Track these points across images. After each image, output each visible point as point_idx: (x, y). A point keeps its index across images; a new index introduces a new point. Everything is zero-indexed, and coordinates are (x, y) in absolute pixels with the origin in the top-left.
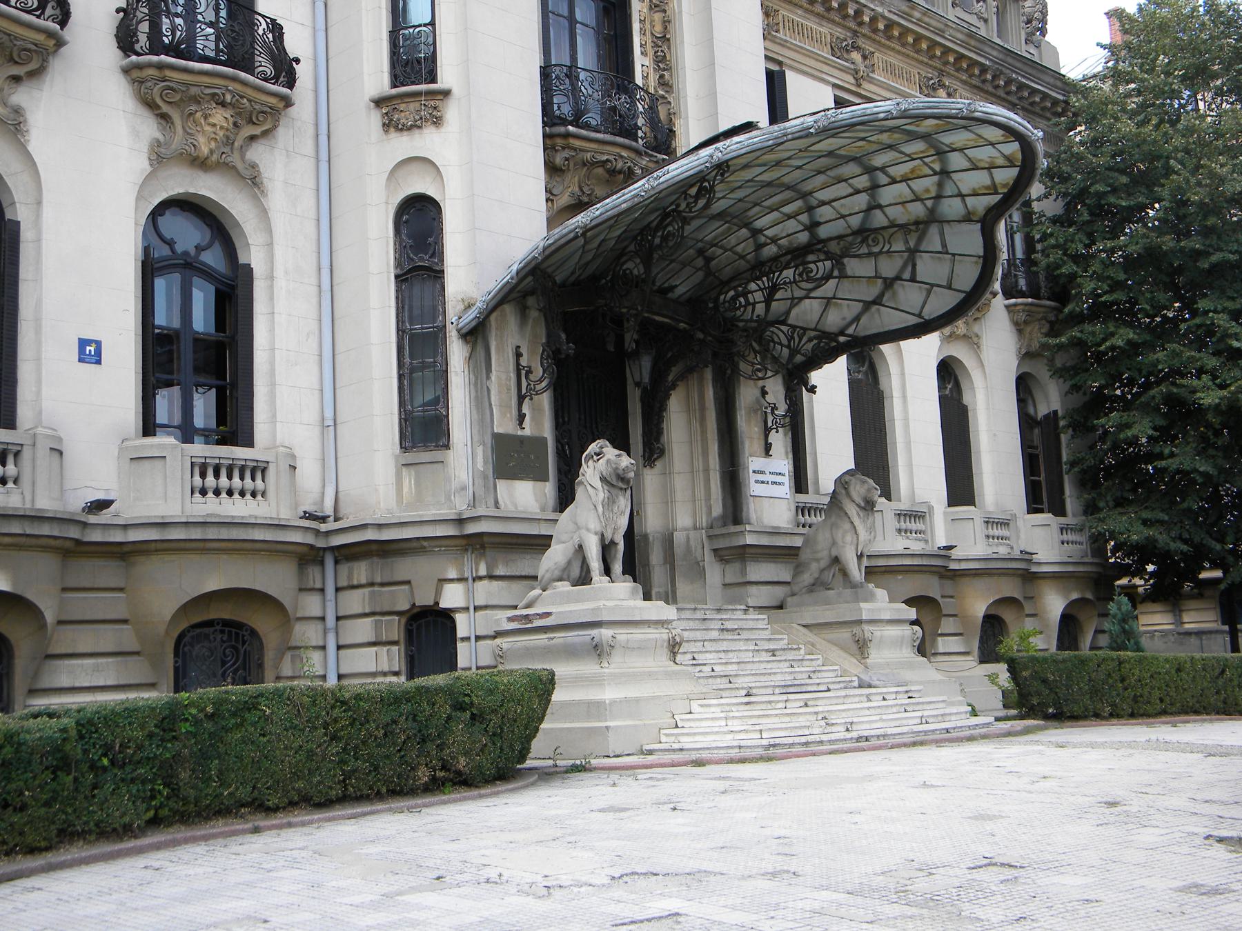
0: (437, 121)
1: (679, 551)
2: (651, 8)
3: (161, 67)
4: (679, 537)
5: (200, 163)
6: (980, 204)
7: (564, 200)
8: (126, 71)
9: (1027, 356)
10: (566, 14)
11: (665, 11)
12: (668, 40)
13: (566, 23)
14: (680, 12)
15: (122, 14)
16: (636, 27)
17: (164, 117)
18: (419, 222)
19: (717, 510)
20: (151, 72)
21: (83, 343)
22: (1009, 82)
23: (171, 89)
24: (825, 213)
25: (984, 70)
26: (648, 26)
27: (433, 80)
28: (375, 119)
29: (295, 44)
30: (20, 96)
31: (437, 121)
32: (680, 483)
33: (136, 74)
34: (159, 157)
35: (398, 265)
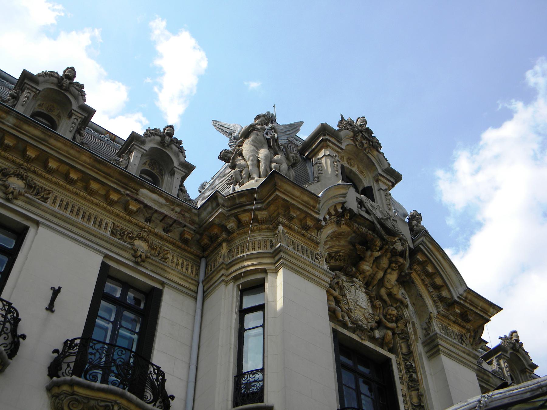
2: (409, 389)
3: (72, 384)
8: (49, 389)
10: (354, 387)
11: (418, 390)
12: (423, 407)
13: (354, 394)
14: (428, 389)
15: (56, 355)
16: (400, 399)
20: (65, 388)
23: (77, 400)
26: (408, 399)
29: (170, 388)
33: (56, 390)
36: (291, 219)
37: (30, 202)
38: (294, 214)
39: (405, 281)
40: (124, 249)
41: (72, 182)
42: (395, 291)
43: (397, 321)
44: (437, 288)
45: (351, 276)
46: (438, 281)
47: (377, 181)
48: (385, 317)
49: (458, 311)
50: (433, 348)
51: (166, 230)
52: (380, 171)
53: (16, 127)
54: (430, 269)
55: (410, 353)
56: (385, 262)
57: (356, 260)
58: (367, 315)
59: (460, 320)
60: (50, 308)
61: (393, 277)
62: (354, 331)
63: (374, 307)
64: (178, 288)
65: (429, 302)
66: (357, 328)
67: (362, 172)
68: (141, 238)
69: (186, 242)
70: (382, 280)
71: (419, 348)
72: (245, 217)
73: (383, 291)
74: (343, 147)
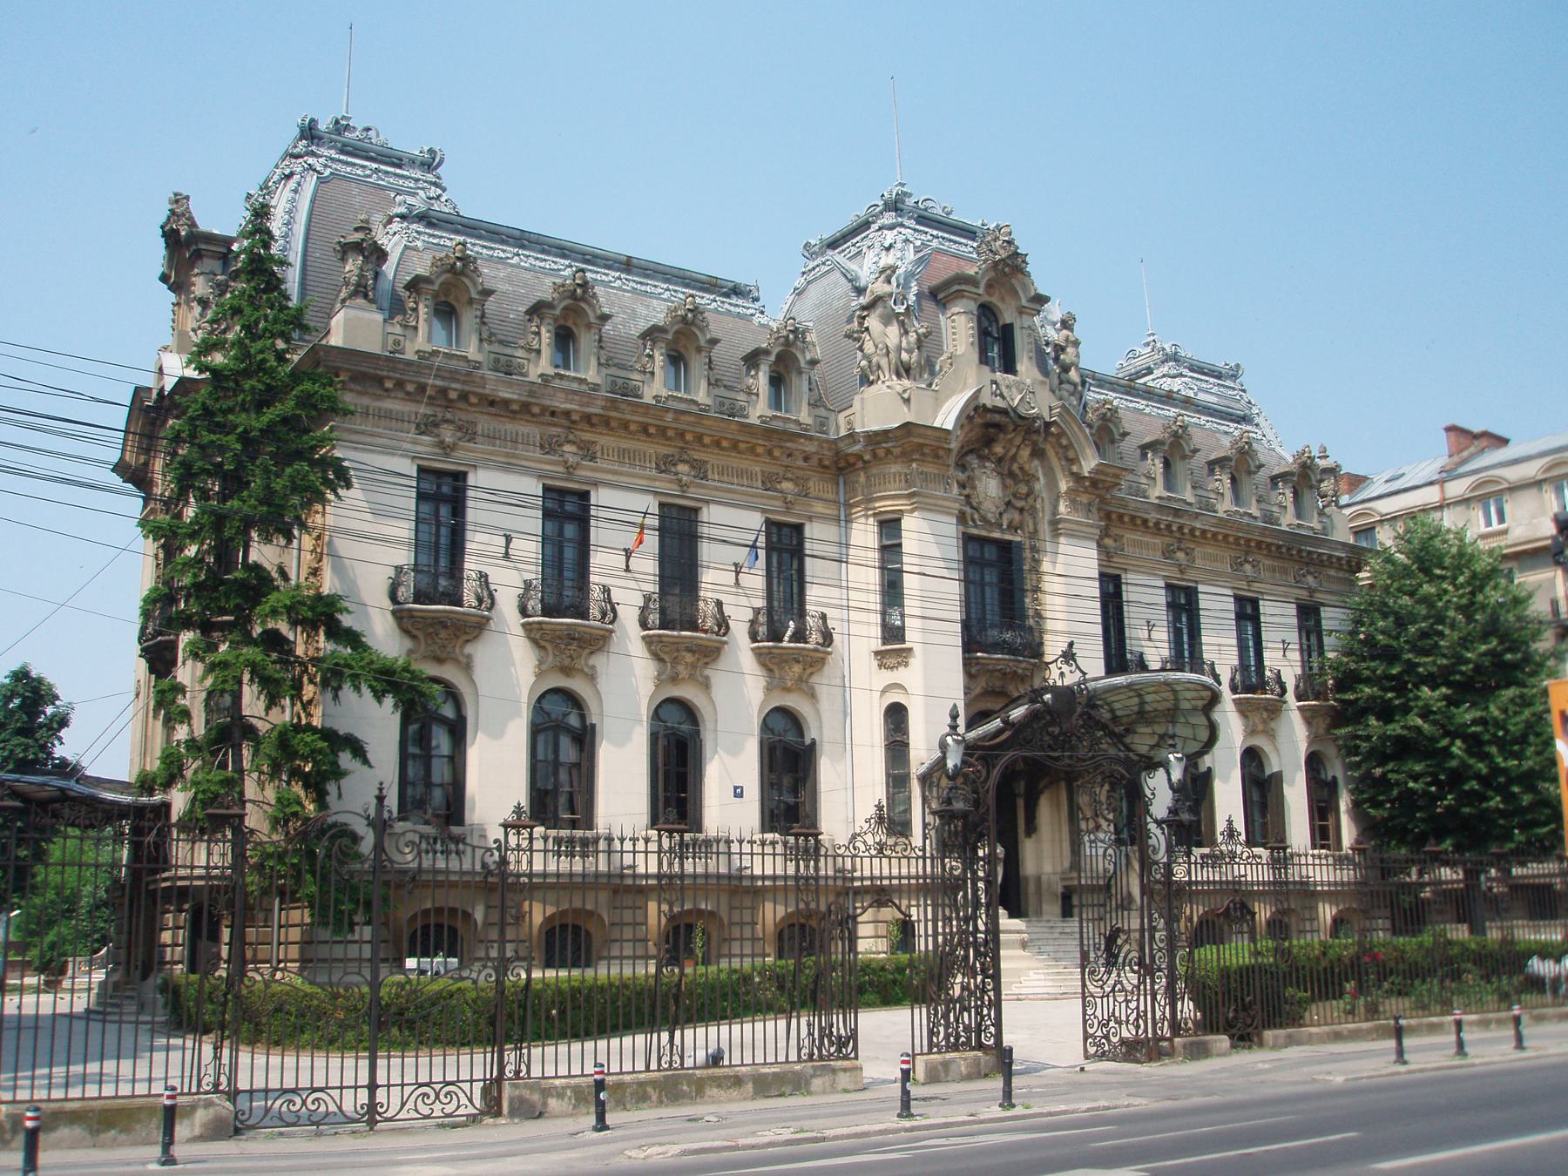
0: (906, 665)
1: (1044, 886)
4: (1044, 878)
5: (787, 690)
6: (1200, 703)
7: (978, 690)
9: (1313, 739)
17: (770, 670)
18: (896, 716)
19: (1067, 864)
21: (736, 788)
22: (1300, 551)
24: (1117, 706)
25: (1279, 547)
27: (904, 641)
28: (875, 663)
31: (906, 665)
32: (1046, 847)
34: (769, 689)
35: (887, 738)
36: (923, 454)
38: (926, 450)
39: (1038, 453)
41: (723, 449)
42: (1027, 467)
43: (1028, 495)
44: (1068, 459)
45: (982, 458)
46: (1071, 454)
47: (1021, 313)
48: (1014, 495)
50: (1056, 533)
52: (1024, 302)
53: (676, 420)
54: (1064, 442)
55: (1036, 531)
56: (1018, 441)
57: (989, 442)
61: (1025, 453)
62: (982, 527)
63: (1005, 487)
64: (823, 518)
67: (1003, 299)
68: (787, 479)
69: (825, 467)
71: (1045, 529)
72: (881, 453)
73: (1015, 467)
74: (981, 291)
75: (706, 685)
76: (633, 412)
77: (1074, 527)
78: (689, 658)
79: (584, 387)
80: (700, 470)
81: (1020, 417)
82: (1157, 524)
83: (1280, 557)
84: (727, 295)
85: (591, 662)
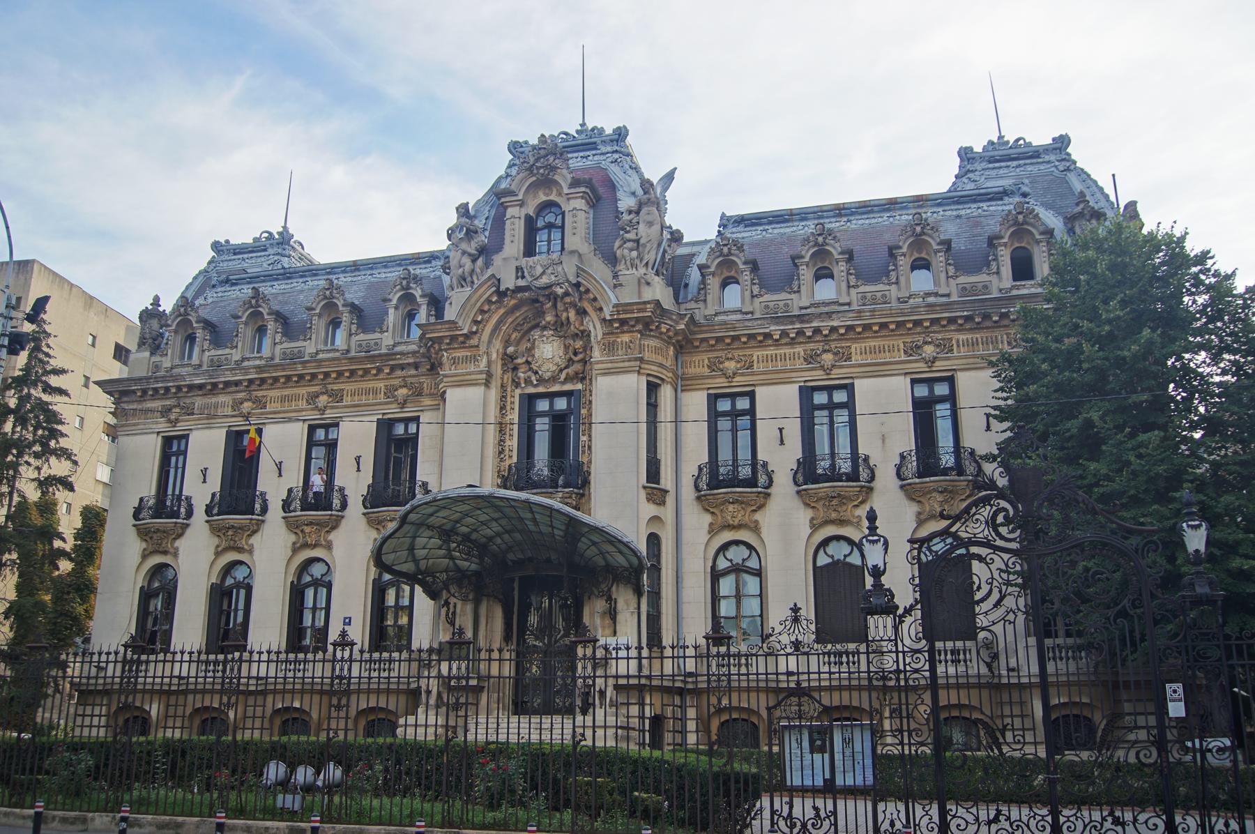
25: (968, 319)
30: (331, 537)
37: (332, 408)
39: (582, 313)
40: (390, 403)
49: (616, 325)
51: (417, 368)
52: (566, 191)
57: (541, 314)
58: (557, 359)
59: (625, 328)
60: (358, 470)
61: (572, 314)
63: (566, 347)
65: (598, 326)
66: (541, 381)
70: (568, 318)
74: (520, 197)
75: (329, 546)
76: (276, 371)
77: (610, 365)
78: (307, 529)
79: (337, 354)
80: (337, 397)
81: (544, 288)
82: (784, 334)
83: (978, 328)
84: (429, 262)
85: (251, 541)
